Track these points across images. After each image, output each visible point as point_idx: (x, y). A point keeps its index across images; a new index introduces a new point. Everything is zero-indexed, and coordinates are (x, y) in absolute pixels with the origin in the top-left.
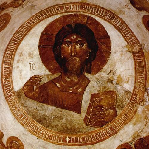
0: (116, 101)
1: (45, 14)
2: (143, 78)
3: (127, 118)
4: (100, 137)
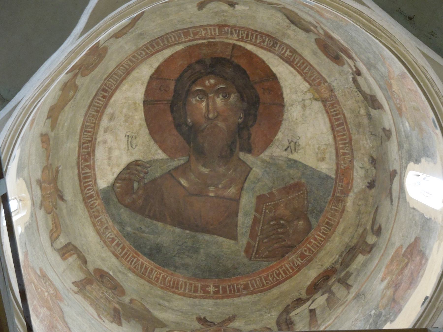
0: (308, 202)
1: (158, 44)
2: (348, 143)
3: (330, 228)
4: (280, 276)
